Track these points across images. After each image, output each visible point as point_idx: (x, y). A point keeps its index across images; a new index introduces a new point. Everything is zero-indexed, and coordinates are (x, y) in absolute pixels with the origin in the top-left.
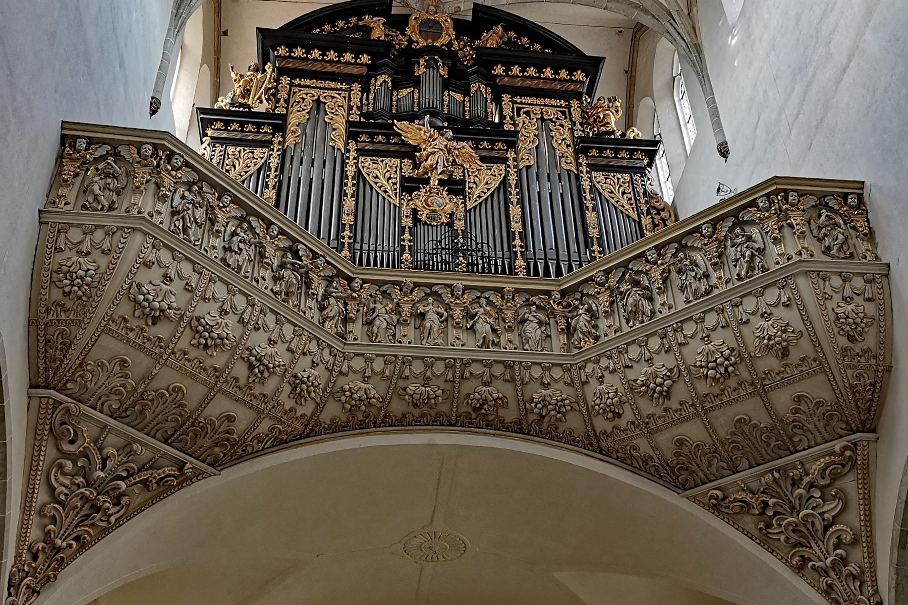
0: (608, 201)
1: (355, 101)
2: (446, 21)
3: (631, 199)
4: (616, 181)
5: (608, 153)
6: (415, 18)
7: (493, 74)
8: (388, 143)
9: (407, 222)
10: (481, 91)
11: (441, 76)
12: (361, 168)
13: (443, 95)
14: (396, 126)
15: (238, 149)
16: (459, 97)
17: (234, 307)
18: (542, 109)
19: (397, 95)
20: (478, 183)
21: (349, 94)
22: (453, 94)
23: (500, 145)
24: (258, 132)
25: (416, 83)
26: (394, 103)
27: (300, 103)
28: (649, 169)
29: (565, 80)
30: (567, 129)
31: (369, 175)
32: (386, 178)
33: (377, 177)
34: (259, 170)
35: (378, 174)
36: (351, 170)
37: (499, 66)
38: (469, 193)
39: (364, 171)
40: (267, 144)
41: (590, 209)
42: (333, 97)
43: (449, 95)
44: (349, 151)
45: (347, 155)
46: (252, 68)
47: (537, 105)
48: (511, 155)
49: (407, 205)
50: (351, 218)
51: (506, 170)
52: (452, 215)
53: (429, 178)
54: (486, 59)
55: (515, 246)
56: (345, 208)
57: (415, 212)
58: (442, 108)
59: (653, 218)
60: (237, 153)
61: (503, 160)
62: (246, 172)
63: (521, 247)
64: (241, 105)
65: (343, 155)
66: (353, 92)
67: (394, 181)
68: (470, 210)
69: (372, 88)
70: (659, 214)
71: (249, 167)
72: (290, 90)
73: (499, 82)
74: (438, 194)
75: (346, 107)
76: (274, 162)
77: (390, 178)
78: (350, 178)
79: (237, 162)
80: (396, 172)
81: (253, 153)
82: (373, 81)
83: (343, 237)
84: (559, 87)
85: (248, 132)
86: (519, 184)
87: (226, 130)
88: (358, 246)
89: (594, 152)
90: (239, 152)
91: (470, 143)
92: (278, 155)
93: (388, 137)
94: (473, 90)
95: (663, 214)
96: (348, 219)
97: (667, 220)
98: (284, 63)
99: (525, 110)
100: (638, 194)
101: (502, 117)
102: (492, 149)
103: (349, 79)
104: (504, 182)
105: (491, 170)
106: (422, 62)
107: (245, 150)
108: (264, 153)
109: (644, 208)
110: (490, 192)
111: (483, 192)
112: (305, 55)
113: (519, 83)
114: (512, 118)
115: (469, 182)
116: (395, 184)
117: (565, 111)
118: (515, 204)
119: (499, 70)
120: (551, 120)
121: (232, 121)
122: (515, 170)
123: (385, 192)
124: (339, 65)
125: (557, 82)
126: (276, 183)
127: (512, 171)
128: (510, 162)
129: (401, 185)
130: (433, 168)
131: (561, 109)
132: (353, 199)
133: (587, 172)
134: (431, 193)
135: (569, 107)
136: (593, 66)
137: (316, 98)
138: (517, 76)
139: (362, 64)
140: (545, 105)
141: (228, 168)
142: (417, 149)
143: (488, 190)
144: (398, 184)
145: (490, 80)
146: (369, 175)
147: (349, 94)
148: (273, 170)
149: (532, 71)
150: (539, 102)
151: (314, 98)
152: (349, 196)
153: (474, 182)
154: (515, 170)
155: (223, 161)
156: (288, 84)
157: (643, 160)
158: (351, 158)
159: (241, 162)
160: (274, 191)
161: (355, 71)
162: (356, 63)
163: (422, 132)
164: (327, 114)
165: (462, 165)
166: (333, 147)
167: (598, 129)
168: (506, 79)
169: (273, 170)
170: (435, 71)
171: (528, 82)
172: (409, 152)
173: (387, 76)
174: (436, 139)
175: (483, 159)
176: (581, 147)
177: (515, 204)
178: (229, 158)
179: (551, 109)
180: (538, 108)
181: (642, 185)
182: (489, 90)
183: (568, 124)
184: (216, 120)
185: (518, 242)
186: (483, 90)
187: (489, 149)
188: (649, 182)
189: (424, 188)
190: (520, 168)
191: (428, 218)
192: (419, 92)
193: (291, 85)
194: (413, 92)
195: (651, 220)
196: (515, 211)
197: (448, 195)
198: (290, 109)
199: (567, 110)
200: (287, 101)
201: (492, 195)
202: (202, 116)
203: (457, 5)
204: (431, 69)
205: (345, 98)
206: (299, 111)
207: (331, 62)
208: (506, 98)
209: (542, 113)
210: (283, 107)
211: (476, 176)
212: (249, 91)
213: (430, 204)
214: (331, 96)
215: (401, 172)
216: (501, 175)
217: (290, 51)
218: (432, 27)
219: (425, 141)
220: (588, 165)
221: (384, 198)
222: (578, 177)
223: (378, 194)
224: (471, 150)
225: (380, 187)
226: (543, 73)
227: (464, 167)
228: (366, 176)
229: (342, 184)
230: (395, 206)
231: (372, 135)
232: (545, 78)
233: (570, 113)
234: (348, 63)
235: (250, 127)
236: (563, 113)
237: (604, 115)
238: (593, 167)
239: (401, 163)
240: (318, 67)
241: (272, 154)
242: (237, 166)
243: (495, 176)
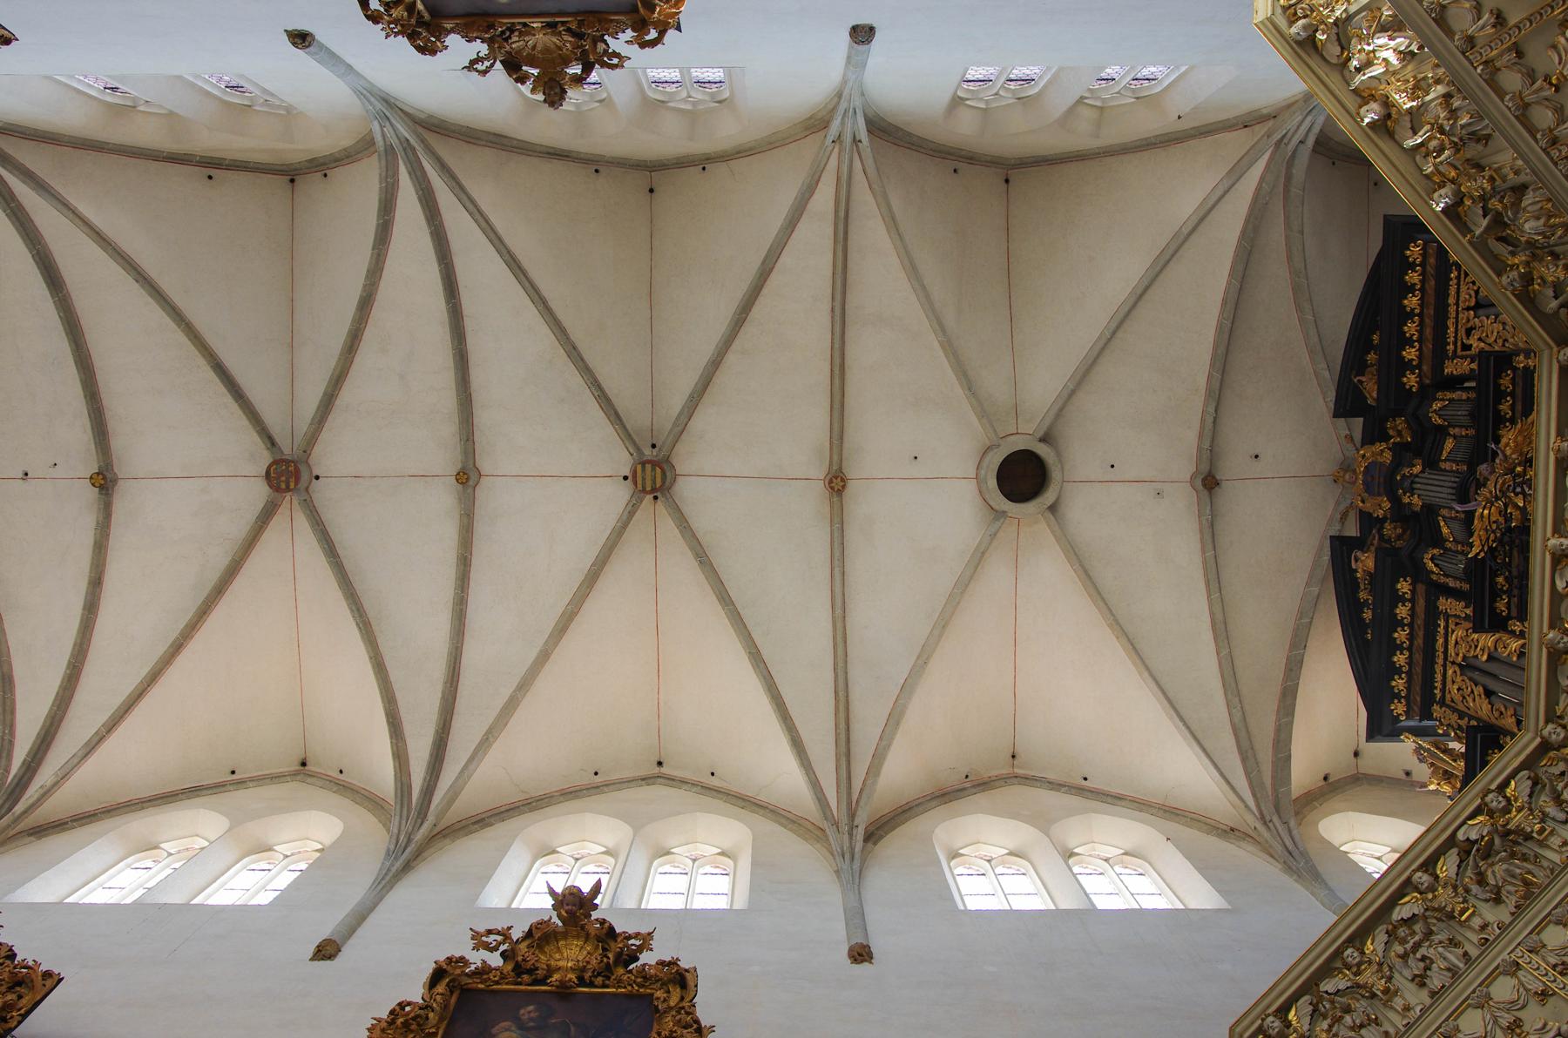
2: (1364, 456)
6: (1363, 502)
7: (1418, 389)
10: (1440, 409)
13: (1445, 470)
16: (1449, 444)
17: (1511, 1005)
23: (1505, 382)
29: (1423, 274)
42: (1457, 643)
43: (1445, 460)
47: (1457, 318)
69: (1443, 579)
72: (1448, 706)
84: (1433, 283)
98: (1415, 708)
112: (1403, 676)
119: (1411, 380)
120: (1477, 292)
124: (1416, 626)
125: (1427, 286)
137: (1457, 669)
138: (1420, 350)
139: (1413, 591)
140: (1457, 304)
145: (1426, 393)
150: (1453, 315)
161: (1421, 603)
162: (1412, 601)
164: (1477, 656)
168: (1425, 368)
170: (1417, 480)
171: (1428, 332)
180: (1461, 316)
182: (1439, 395)
193: (1442, 703)
194: (1444, 517)
198: (1471, 712)
203: (1343, 438)
204: (1415, 486)
205: (1457, 624)
206: (1474, 700)
207: (1411, 637)
209: (1468, 309)
212: (1446, 772)
217: (1398, 696)
218: (1372, 477)
226: (1413, 310)
232: (1421, 305)
240: (1418, 657)
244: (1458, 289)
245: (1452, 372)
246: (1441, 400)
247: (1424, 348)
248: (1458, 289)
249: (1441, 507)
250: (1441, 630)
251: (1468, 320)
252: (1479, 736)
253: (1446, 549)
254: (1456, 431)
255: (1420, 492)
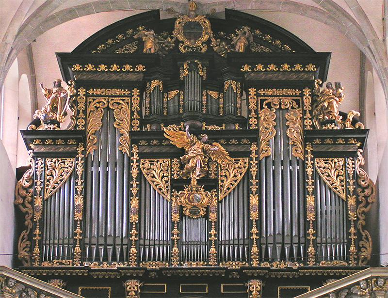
0: (325, 184)
1: (136, 105)
3: (342, 181)
4: (333, 165)
5: (328, 141)
7: (241, 71)
8: (161, 145)
9: (176, 217)
11: (202, 76)
12: (142, 169)
13: (202, 95)
14: (166, 133)
15: (54, 160)
16: (214, 94)
18: (280, 99)
19: (167, 97)
20: (228, 175)
21: (131, 99)
22: (210, 92)
23: (245, 141)
24: (66, 144)
25: (181, 85)
26: (165, 105)
27: (95, 112)
28: (361, 151)
30: (299, 118)
31: (148, 175)
32: (161, 177)
33: (154, 177)
34: (70, 177)
35: (154, 173)
36: (135, 172)
37: (246, 66)
38: (221, 186)
39: (144, 172)
40: (73, 155)
41: (311, 193)
42: (119, 104)
44: (132, 155)
45: (132, 158)
46: (56, 84)
47: (276, 96)
48: (254, 148)
49: (176, 200)
50: (136, 217)
51: (249, 162)
52: (207, 208)
53: (191, 179)
54: (235, 60)
55: (252, 234)
56: (132, 209)
57: (181, 207)
58: (202, 108)
59: (357, 198)
60: (53, 164)
61: (247, 154)
62: (61, 180)
63: (257, 234)
64: (54, 122)
65: (129, 158)
66: (133, 98)
67: (166, 179)
68: (222, 200)
70: (363, 191)
71: (62, 176)
72: (86, 102)
73: (247, 76)
74: (197, 191)
75: (129, 111)
76: (80, 170)
77: (163, 177)
78: (134, 179)
79: (54, 172)
80: (167, 170)
81: (64, 163)
82: (148, 85)
83: (131, 236)
85: (59, 145)
86: (259, 176)
87: (44, 144)
88: (142, 242)
89: (318, 141)
90: (55, 163)
91: (222, 141)
92: (82, 163)
93: (160, 141)
94: (226, 86)
95: (367, 192)
96: (134, 218)
97: (369, 196)
98: (80, 76)
99: (267, 101)
100: (349, 176)
101: (250, 111)
102: (239, 144)
103: (129, 85)
104: (248, 172)
105: (237, 163)
106: (185, 66)
107: (58, 161)
108: (72, 163)
109: (351, 188)
110: (236, 184)
111: (231, 184)
113: (263, 77)
114: (256, 111)
115: (221, 176)
116: (167, 182)
117: (299, 100)
118: (254, 193)
119: (246, 68)
121: (47, 139)
122: (257, 162)
123: (160, 189)
126: (82, 188)
127: (254, 163)
128: (253, 155)
129: (171, 183)
130: (193, 169)
131: (296, 98)
132: (137, 198)
133: (312, 159)
134: (192, 191)
135: (302, 95)
136: (322, 60)
137: (106, 105)
140: (283, 96)
141: (48, 177)
142: (183, 152)
143: (235, 181)
144: (169, 182)
146: (148, 175)
147: (131, 99)
148: (80, 177)
149: (272, 67)
151: (105, 107)
152: (134, 196)
153: (226, 176)
154: (257, 162)
155: (45, 173)
156: (84, 95)
157: (355, 144)
158: (135, 161)
159: (57, 171)
160: (81, 196)
163: (185, 137)
164: (115, 120)
165: (216, 161)
166: (121, 151)
167: (324, 117)
168: (252, 74)
169: (80, 177)
172: (179, 153)
173: (158, 81)
174: (195, 144)
175: (232, 155)
176: (308, 136)
177: (254, 193)
178: (48, 169)
179: (285, 98)
181: (353, 168)
182: (239, 86)
183: (299, 112)
184: (35, 139)
185: (254, 230)
186: (234, 87)
187: (237, 144)
188: (359, 163)
189: (187, 187)
190: (260, 159)
191: (190, 212)
192: (184, 94)
193: (87, 95)
194: (179, 94)
195: (355, 200)
196: (254, 200)
197: (204, 191)
199: (300, 98)
200: (85, 112)
201: (238, 185)
202: (26, 137)
204: (193, 71)
205: (128, 103)
208: (252, 91)
209: (280, 104)
210: (83, 118)
211: (227, 169)
212: (56, 108)
213: (192, 201)
214: (117, 103)
215: (171, 171)
216: (245, 167)
219: (187, 143)
220: (313, 153)
221: (159, 195)
222: (304, 166)
223: (155, 191)
224: (222, 148)
225: (156, 186)
226: (282, 68)
227: (218, 163)
228: (146, 176)
229: (130, 186)
230: (167, 201)
231: (149, 141)
232: (284, 71)
233: (303, 103)
234: (128, 72)
235: (59, 142)
236: (297, 102)
237: (329, 103)
238: (317, 155)
239: (171, 162)
240: (105, 77)
241: (78, 164)
242: (54, 175)
243: (241, 168)
244: (289, 96)
245: (250, 94)
246: (236, 86)
247: (262, 74)
248: (289, 96)
249: (184, 92)
250: (123, 92)
251: (275, 105)
252: (81, 137)
253: (163, 95)
254: (221, 101)
255: (190, 74)
